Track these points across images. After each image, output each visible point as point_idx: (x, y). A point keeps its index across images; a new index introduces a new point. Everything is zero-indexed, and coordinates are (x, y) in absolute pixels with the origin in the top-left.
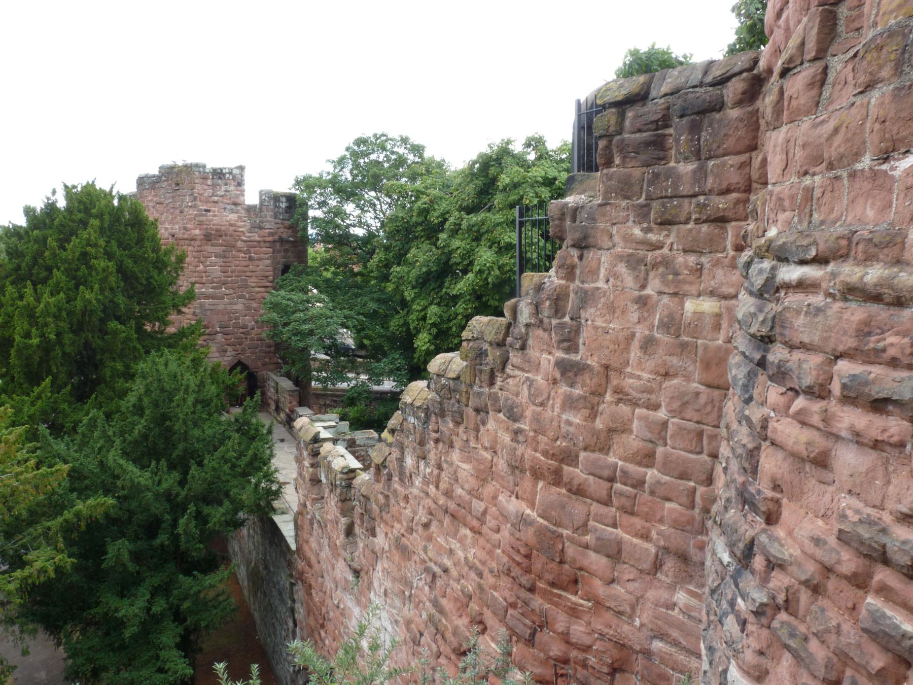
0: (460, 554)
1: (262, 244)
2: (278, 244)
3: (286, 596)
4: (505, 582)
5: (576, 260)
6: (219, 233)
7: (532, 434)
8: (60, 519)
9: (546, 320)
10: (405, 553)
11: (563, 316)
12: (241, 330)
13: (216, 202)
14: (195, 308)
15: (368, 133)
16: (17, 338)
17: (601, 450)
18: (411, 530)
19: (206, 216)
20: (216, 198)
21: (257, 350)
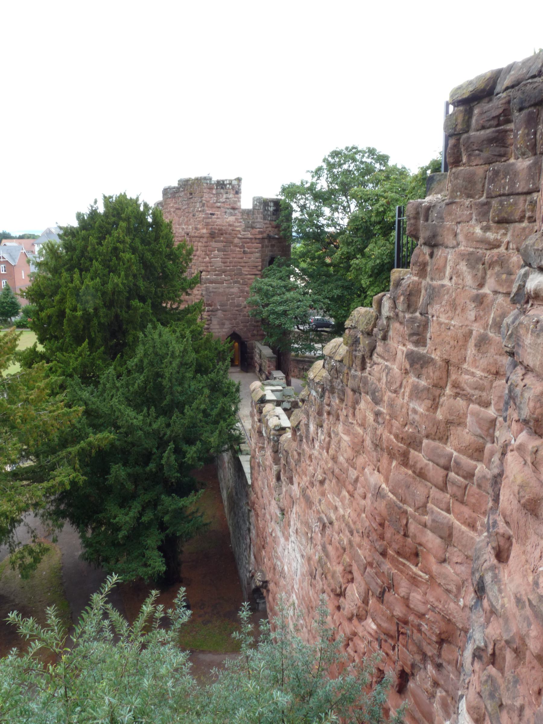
0: (341, 511)
1: (253, 241)
2: (266, 241)
3: (246, 518)
4: (366, 543)
5: (428, 257)
6: (221, 232)
7: (388, 417)
8: (78, 447)
9: (401, 314)
10: (309, 503)
11: (415, 311)
12: (236, 308)
13: (219, 207)
14: (202, 290)
15: (341, 147)
16: (67, 310)
17: (440, 439)
18: (312, 484)
19: (211, 218)
20: (219, 204)
21: (248, 324)
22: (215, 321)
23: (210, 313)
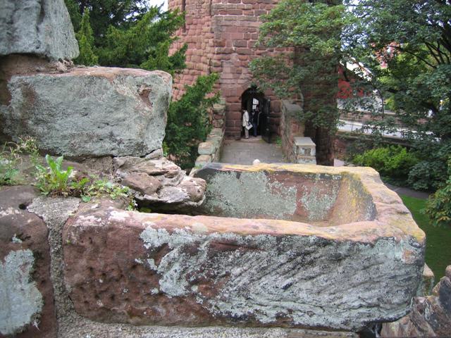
12: (258, 51)
22: (227, 69)
23: (220, 56)
